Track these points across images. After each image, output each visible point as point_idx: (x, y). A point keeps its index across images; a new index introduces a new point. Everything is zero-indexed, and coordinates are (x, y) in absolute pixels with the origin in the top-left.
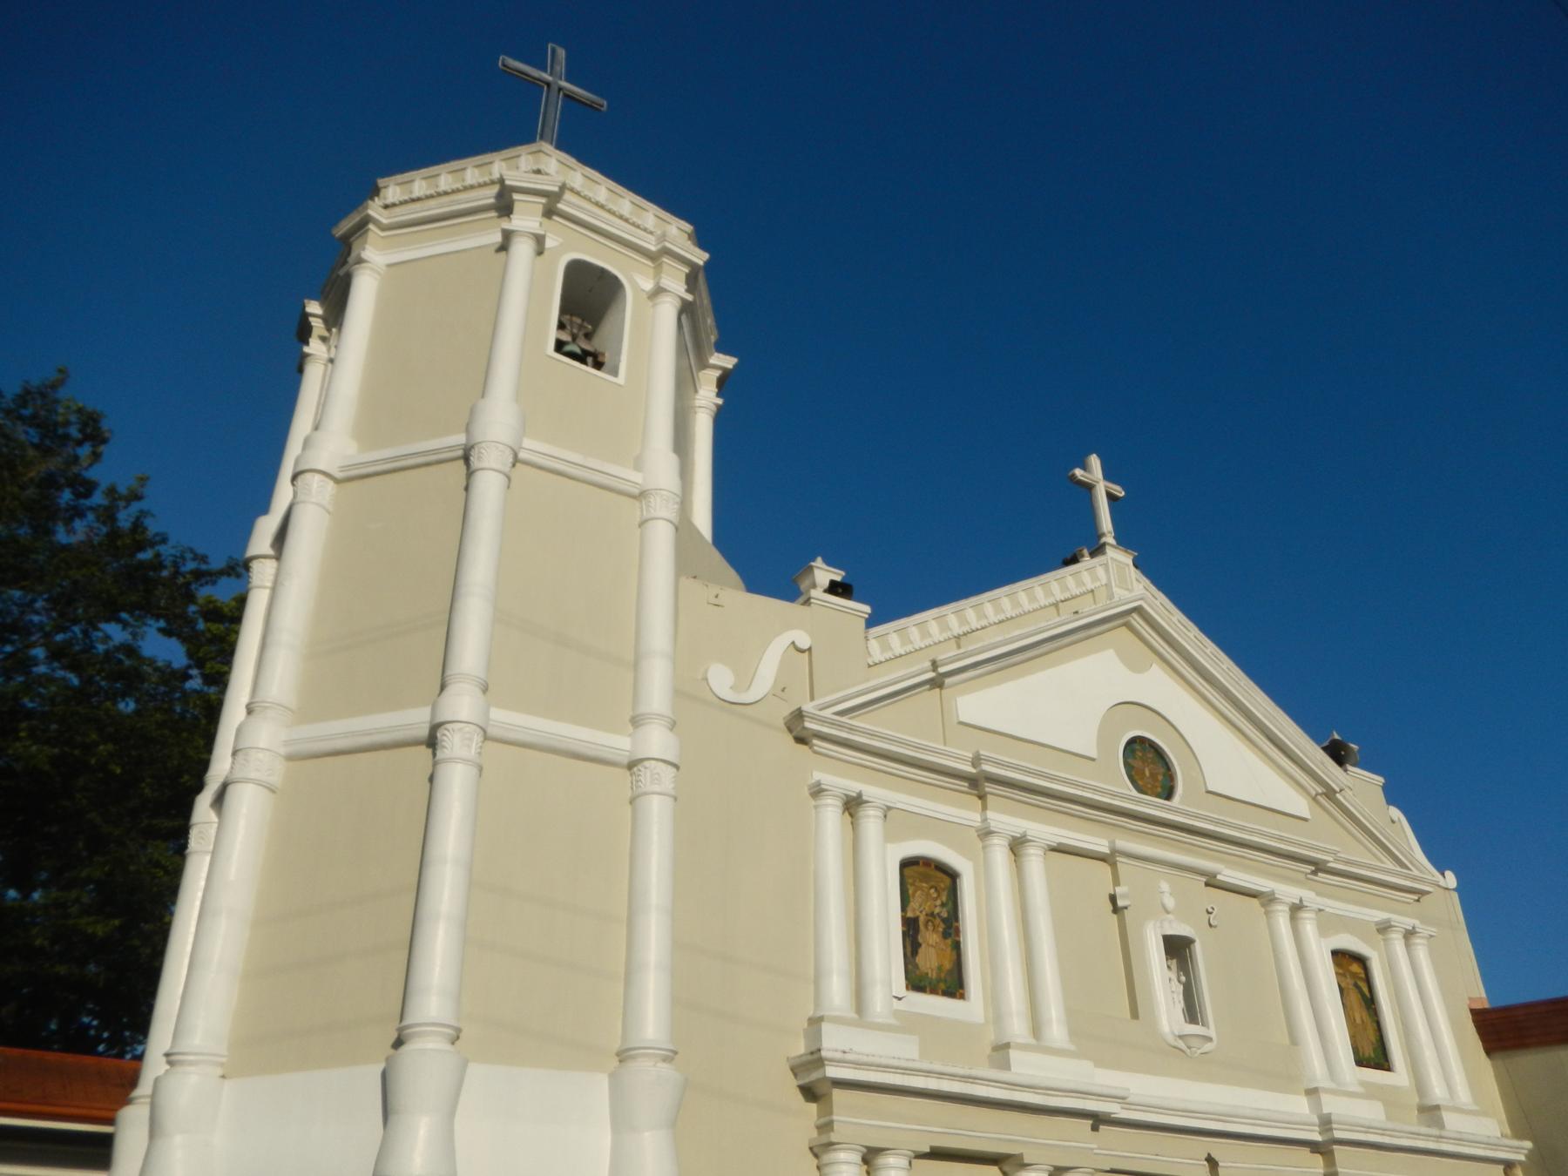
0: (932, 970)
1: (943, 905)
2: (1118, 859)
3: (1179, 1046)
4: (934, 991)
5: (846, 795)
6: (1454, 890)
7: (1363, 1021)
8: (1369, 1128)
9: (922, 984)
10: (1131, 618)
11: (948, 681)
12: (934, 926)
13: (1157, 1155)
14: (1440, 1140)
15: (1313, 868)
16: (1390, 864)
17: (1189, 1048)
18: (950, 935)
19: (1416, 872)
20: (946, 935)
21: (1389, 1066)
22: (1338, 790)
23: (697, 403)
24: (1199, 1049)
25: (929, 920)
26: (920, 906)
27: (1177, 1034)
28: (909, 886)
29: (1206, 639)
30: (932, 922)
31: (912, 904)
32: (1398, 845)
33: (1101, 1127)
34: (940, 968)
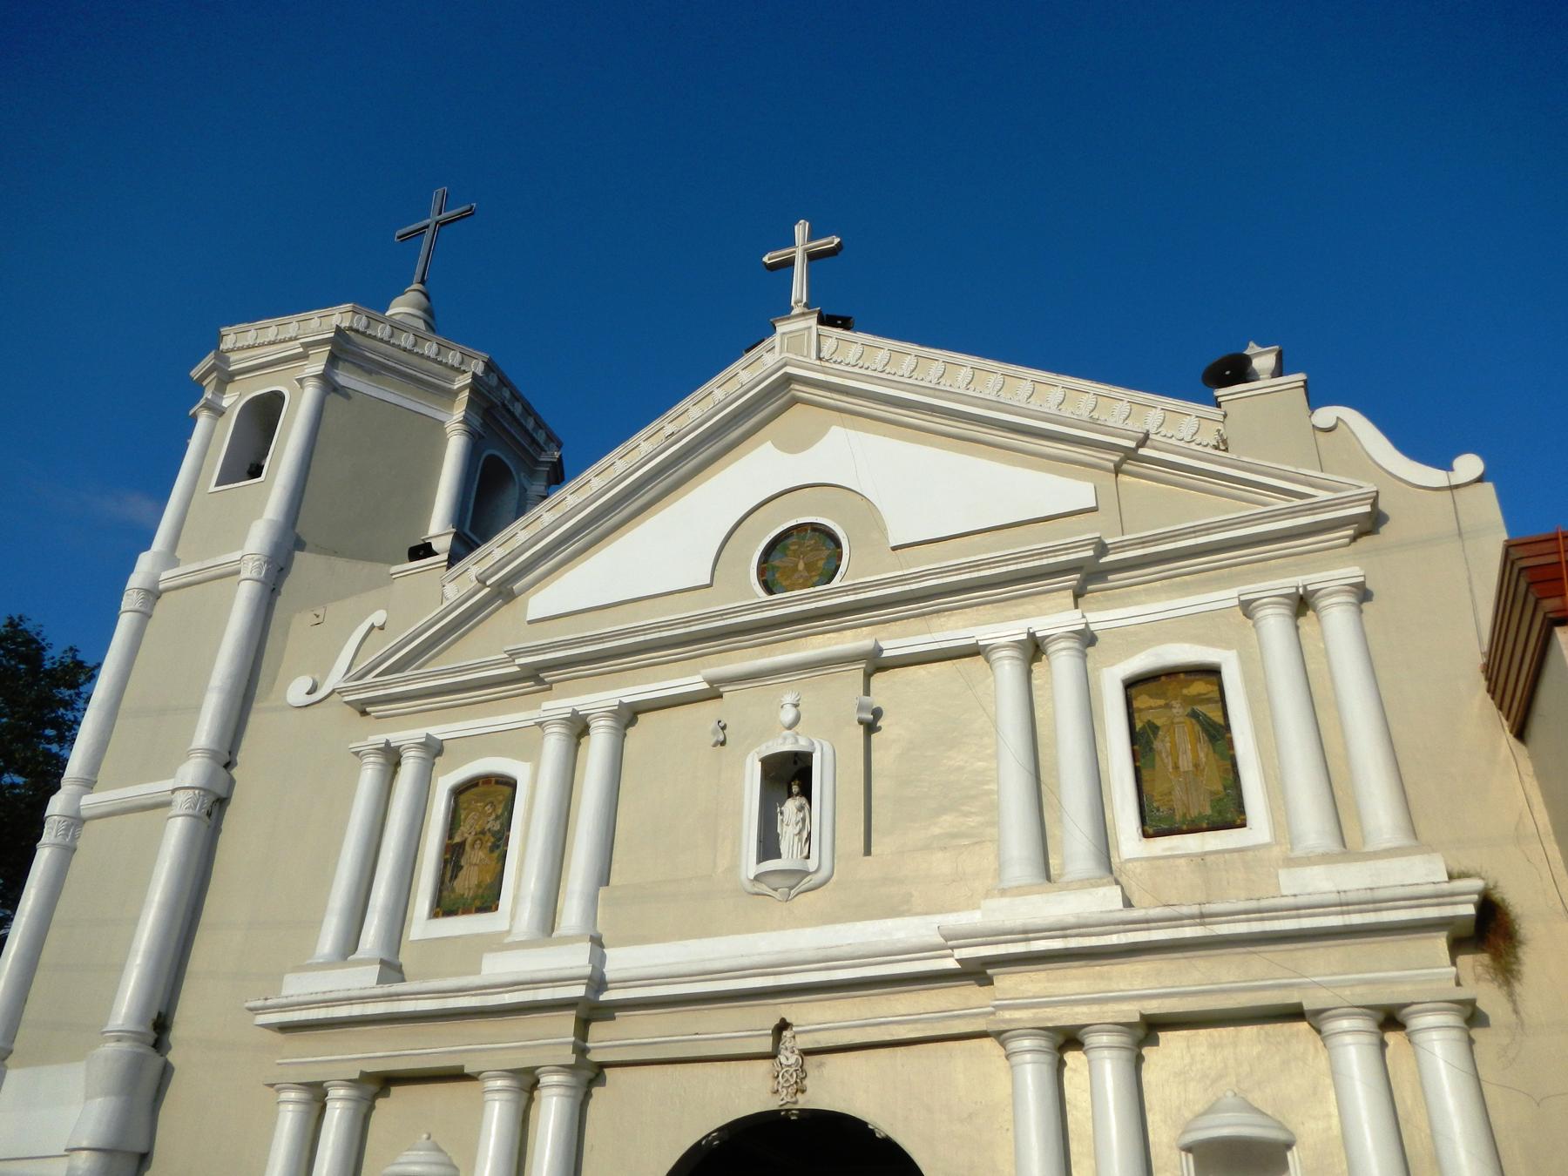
0: (469, 889)
1: (497, 818)
2: (721, 690)
3: (761, 891)
4: (466, 911)
5: (377, 749)
6: (1480, 480)
7: (1196, 766)
8: (1025, 932)
9: (454, 908)
10: (793, 392)
11: (517, 587)
12: (482, 843)
13: (697, 1034)
14: (1207, 920)
15: (1078, 576)
16: (1281, 503)
17: (775, 890)
18: (498, 847)
19: (1323, 495)
20: (492, 850)
21: (1245, 820)
22: (1132, 444)
23: (448, 430)
24: (791, 888)
25: (476, 841)
26: (471, 827)
27: (752, 878)
28: (462, 811)
29: (932, 350)
30: (481, 840)
31: (462, 828)
32: (1277, 472)
33: (616, 1014)
34: (479, 886)
